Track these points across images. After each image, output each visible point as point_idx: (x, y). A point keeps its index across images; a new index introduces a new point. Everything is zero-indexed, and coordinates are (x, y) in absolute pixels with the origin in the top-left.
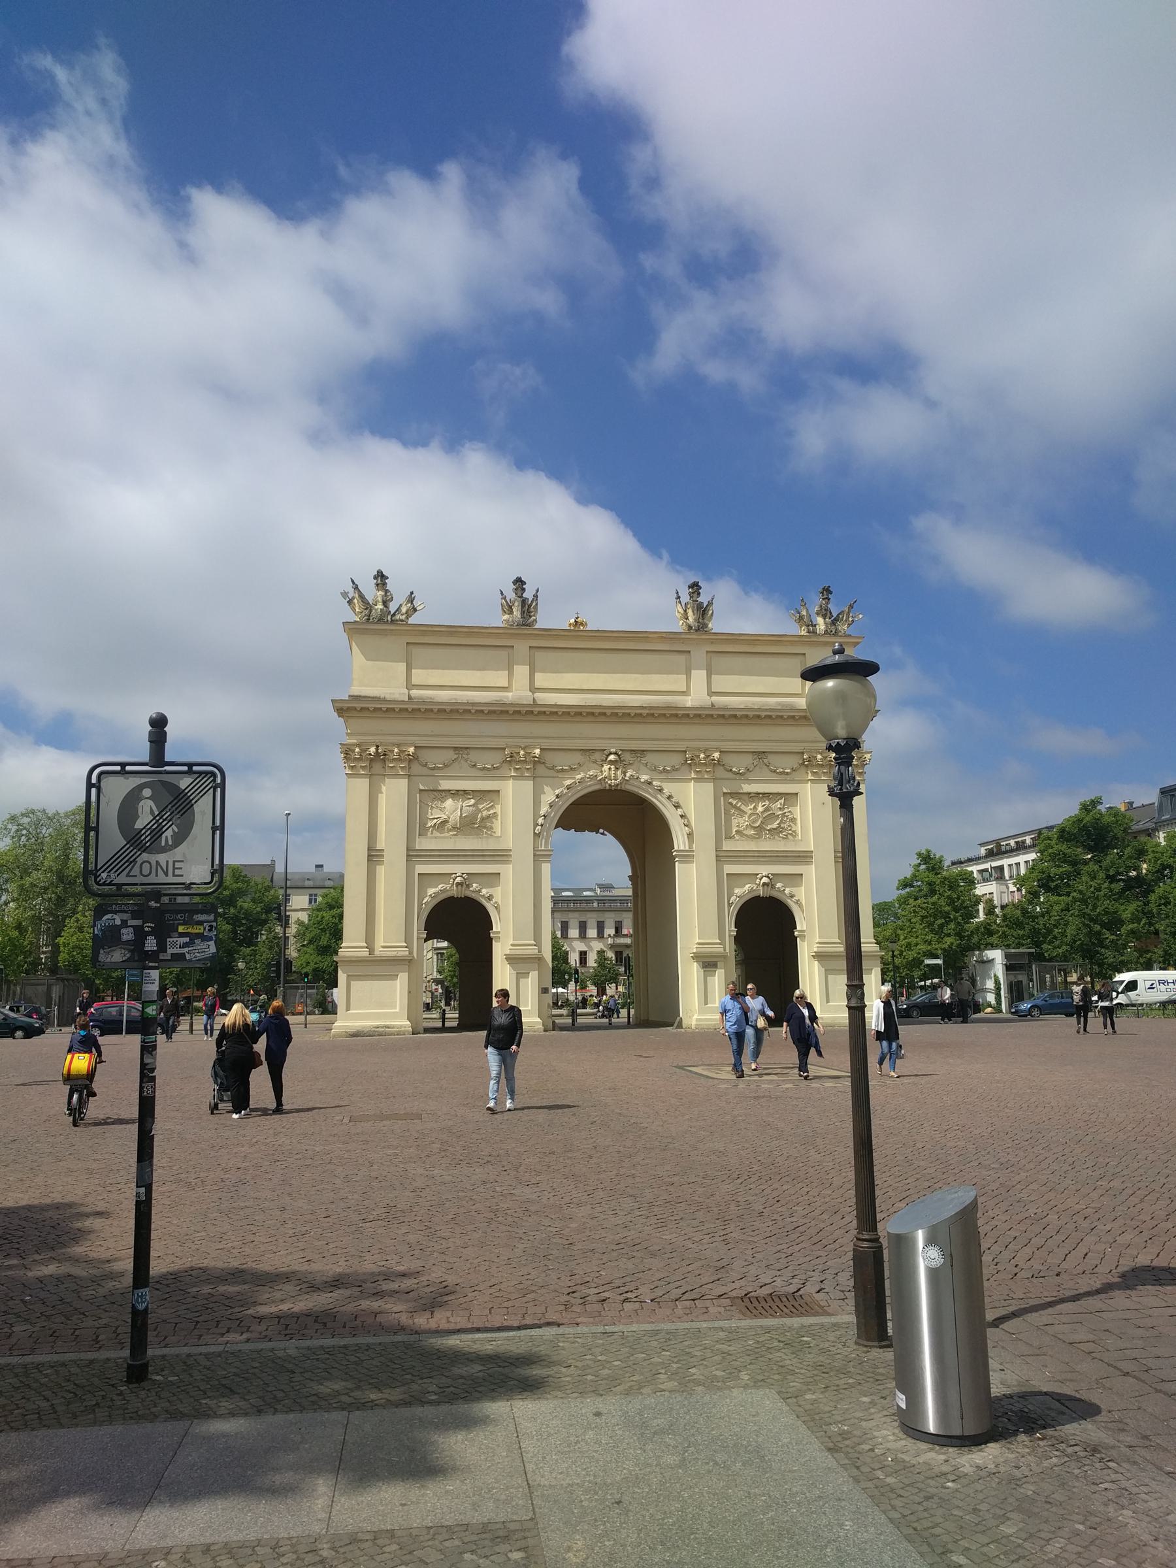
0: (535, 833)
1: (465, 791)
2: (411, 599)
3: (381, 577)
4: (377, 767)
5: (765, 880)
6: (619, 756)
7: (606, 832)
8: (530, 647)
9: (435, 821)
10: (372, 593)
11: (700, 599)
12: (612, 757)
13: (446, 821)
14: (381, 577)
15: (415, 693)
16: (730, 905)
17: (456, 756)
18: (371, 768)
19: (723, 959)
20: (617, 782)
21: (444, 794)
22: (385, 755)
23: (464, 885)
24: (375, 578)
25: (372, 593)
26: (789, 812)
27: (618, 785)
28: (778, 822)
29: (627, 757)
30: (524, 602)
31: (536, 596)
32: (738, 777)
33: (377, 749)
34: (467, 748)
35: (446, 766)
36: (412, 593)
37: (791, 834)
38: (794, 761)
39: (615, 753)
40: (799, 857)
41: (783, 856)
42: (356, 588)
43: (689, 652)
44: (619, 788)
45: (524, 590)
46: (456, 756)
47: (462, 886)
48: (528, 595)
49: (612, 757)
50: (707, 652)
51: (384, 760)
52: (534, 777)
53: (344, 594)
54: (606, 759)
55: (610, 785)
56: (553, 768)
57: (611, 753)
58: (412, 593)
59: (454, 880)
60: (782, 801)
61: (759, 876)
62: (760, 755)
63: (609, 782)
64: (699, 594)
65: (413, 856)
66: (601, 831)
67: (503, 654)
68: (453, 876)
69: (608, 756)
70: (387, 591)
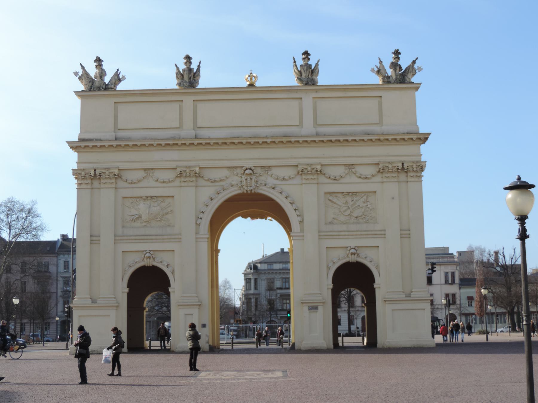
0: (196, 223)
1: (151, 197)
2: (117, 74)
3: (99, 61)
4: (96, 183)
5: (353, 251)
6: (253, 170)
7: (273, 219)
8: (194, 101)
9: (133, 217)
10: (93, 71)
11: (309, 63)
12: (248, 172)
13: (140, 217)
14: (99, 61)
15: (120, 134)
16: (328, 268)
17: (145, 175)
18: (92, 184)
19: (322, 304)
20: (251, 188)
21: (138, 199)
22: (100, 175)
23: (151, 258)
24: (95, 61)
25: (93, 71)
26: (370, 204)
27: (252, 190)
28: (363, 210)
29: (258, 171)
30: (190, 70)
31: (199, 66)
32: (335, 181)
33: (95, 172)
34: (152, 169)
35: (139, 181)
36: (118, 70)
37: (371, 219)
38: (372, 170)
39: (250, 169)
40: (376, 235)
41: (365, 235)
42: (83, 68)
43: (301, 98)
44: (253, 192)
45: (191, 63)
46: (145, 175)
47: (150, 259)
48: (194, 66)
49: (248, 172)
50: (313, 98)
51: (99, 179)
52: (196, 186)
53: (76, 74)
54: (244, 172)
55: (246, 190)
56: (209, 180)
57: (247, 169)
58: (118, 70)
59: (145, 255)
60: (365, 197)
61: (349, 248)
62: (350, 166)
63: (246, 188)
64: (309, 59)
65: (118, 239)
66: (269, 218)
67: (177, 106)
68: (145, 252)
69: (245, 171)
70: (103, 70)
